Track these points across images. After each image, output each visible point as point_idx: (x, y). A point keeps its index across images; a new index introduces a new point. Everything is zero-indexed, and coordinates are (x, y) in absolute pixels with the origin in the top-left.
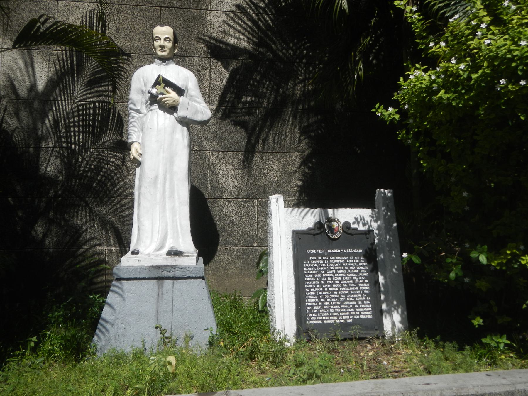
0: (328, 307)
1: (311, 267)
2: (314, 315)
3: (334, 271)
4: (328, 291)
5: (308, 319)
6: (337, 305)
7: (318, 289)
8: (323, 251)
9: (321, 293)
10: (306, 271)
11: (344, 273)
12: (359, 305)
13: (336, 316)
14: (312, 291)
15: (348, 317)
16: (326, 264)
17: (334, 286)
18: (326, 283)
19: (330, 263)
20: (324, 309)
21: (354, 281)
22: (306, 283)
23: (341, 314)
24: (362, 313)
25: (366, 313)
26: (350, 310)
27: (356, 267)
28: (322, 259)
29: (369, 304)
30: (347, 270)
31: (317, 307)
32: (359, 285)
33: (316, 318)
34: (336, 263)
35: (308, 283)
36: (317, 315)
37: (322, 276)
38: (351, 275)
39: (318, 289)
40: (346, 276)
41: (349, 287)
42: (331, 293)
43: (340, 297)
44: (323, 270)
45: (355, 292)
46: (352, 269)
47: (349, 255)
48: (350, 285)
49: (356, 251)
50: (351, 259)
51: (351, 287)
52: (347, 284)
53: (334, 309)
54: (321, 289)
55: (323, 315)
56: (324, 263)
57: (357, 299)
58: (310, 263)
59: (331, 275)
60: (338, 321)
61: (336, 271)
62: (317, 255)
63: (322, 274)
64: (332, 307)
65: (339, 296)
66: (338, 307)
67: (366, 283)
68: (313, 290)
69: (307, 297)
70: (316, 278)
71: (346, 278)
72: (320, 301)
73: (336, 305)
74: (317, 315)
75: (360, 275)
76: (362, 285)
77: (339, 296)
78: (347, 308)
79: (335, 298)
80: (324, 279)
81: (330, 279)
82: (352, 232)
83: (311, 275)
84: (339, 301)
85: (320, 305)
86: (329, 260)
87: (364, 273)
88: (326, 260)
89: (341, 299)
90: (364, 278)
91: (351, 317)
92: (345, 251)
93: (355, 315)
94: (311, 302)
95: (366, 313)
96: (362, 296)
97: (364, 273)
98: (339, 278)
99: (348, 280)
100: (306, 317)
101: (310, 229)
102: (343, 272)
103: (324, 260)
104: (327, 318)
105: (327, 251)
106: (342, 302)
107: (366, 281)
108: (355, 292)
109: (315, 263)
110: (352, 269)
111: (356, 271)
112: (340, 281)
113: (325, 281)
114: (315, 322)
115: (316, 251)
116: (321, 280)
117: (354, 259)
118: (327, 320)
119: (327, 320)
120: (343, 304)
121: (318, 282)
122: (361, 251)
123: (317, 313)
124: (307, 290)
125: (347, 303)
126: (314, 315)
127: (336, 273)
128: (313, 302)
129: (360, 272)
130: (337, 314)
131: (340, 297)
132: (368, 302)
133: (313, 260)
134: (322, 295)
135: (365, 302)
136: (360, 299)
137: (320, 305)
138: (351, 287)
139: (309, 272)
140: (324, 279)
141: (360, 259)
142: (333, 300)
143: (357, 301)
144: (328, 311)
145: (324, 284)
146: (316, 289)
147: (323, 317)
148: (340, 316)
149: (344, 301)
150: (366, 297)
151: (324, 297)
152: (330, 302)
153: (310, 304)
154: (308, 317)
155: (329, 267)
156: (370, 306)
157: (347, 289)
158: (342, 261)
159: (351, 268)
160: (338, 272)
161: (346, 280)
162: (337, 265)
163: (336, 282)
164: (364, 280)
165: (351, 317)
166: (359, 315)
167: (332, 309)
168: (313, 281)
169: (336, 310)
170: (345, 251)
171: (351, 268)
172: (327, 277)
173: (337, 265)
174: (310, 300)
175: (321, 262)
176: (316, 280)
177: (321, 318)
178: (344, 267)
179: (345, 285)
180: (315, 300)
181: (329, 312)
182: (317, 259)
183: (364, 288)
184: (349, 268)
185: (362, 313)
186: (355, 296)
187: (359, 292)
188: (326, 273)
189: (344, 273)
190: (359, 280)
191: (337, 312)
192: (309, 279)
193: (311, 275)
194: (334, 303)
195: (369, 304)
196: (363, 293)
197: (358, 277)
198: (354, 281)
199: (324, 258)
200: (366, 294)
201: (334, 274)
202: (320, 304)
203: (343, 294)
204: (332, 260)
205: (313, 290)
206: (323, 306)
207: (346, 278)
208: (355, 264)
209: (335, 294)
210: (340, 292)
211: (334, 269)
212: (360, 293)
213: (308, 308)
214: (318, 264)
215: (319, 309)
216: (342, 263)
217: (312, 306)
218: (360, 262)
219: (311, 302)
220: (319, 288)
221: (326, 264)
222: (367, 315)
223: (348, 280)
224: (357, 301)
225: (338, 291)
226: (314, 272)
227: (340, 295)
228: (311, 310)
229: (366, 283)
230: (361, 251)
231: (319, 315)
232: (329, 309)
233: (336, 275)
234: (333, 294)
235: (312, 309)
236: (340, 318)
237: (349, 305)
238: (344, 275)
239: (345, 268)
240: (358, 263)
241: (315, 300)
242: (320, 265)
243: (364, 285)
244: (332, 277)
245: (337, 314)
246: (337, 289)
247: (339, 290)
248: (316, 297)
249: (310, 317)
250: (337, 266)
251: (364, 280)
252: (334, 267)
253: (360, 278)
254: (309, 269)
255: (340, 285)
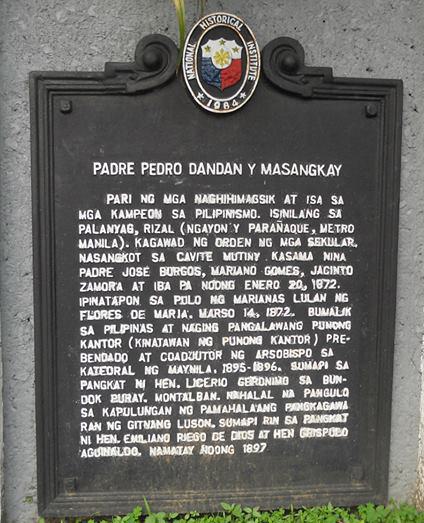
0: (172, 397)
1: (110, 237)
2: (111, 426)
3: (209, 255)
4: (177, 333)
5: (84, 440)
6: (210, 390)
7: (134, 328)
8: (167, 168)
9: (147, 343)
10: (86, 251)
11: (249, 263)
12: (299, 390)
13: (198, 430)
14: (109, 336)
15: (250, 434)
16: (175, 224)
17: (202, 314)
18: (168, 304)
19: (191, 219)
20: (151, 402)
21: (289, 294)
22: (83, 302)
23: (223, 423)
24: (307, 419)
25: (323, 419)
26: (260, 409)
27: (304, 237)
28: (158, 204)
29: (340, 386)
30: (265, 252)
31: (127, 398)
32: (311, 312)
33: (120, 437)
34: (221, 220)
35: (94, 301)
36: (124, 425)
37: (155, 276)
38: (279, 271)
39: (134, 328)
40: (260, 276)
41: (268, 321)
42: (187, 342)
43: (227, 358)
44: (159, 250)
45: (288, 340)
46: (285, 249)
47: (278, 186)
48: (271, 312)
49: (311, 170)
50: (287, 207)
51: (276, 320)
52: (261, 308)
53: (196, 406)
54: (148, 328)
55: (147, 425)
56: (167, 219)
57: (294, 366)
58: (107, 220)
59: (196, 271)
60: (206, 450)
61: (218, 253)
62: (136, 185)
63: (155, 268)
64: (186, 397)
65: (219, 354)
66: (214, 396)
67: (341, 305)
68: (112, 328)
69: (85, 358)
70: (128, 283)
71: (258, 285)
72: (140, 375)
73: (203, 390)
74: (124, 425)
75: (319, 270)
76: (323, 312)
77: (219, 354)
78: (248, 403)
79: (204, 363)
80: (160, 286)
81: (188, 285)
82: (305, 90)
83: (102, 271)
84: (219, 375)
85: (139, 391)
86: (190, 207)
87: (336, 263)
88: (179, 206)
89: (227, 368)
90: (332, 284)
91: (263, 434)
92: (266, 170)
93: (282, 425)
94: (99, 378)
95: (323, 419)
96: (317, 357)
97: (336, 263)
98: (229, 285)
99: (265, 292)
100: (77, 433)
101: (114, 71)
102: (249, 257)
103: (167, 209)
104: (165, 438)
105: (186, 169)
106: (233, 379)
107: (340, 298)
108: (288, 340)
109: (126, 221)
110: (285, 249)
111: (302, 257)
112: (228, 295)
113: (168, 297)
114: (113, 452)
115: (137, 168)
116: (149, 290)
117: (299, 206)
118: (161, 445)
119: (161, 445)
120: (233, 386)
121: (136, 300)
122: (334, 170)
123: (124, 420)
124: (83, 331)
125: (252, 381)
126: (111, 426)
127: (218, 260)
128: (109, 378)
129: (319, 260)
130: (207, 423)
131: (227, 358)
132: (338, 379)
133: (119, 207)
134: (148, 349)
135: (327, 380)
136: (307, 366)
137: (139, 391)
138: (276, 320)
139: (98, 254)
140: (160, 286)
141: (327, 205)
142: (196, 369)
143: (294, 376)
144: (169, 411)
145: (159, 307)
146: (124, 328)
147: (145, 433)
148: (218, 429)
149: (239, 374)
150: (332, 361)
151: (155, 360)
152: (180, 379)
153: (98, 385)
154: (85, 434)
155: (189, 238)
156: (346, 392)
157: (258, 327)
158: (247, 214)
159: (283, 243)
160: (226, 257)
161: (256, 292)
162: (224, 228)
163: (214, 300)
164: (331, 294)
165: (263, 434)
166: (297, 428)
167: (186, 403)
168: (112, 293)
169: (203, 408)
170: (266, 170)
171: (283, 243)
172: (174, 281)
173: (224, 228)
174: (100, 371)
175: (157, 214)
176: (127, 291)
177: (138, 439)
178: (255, 237)
179: (251, 313)
180: (116, 371)
181: (175, 417)
182: (136, 204)
183: (330, 325)
184: (276, 242)
185: (307, 419)
186: (290, 354)
187: (307, 339)
188: (171, 260)
189: (249, 263)
190: (312, 292)
191: (205, 416)
192: (98, 288)
193: (102, 271)
194: (197, 383)
195: (340, 386)
196: (323, 343)
197: (307, 281)
198: (289, 294)
199: (167, 200)
200: (336, 346)
201: (205, 266)
202: (140, 384)
203: (238, 347)
204: (203, 206)
205: (112, 328)
206: (150, 391)
207: (258, 285)
208: (304, 228)
209: (206, 348)
210: (225, 340)
211: (211, 246)
212: (310, 346)
213: (87, 399)
214: (138, 223)
215: (135, 406)
216: (244, 222)
217: (106, 395)
218: (324, 219)
219: (99, 378)
220: (137, 322)
221: (175, 224)
222: (329, 425)
223: (265, 292)
224: (294, 376)
225: (217, 337)
226: (120, 258)
227: (227, 350)
228: (97, 408)
229: (341, 305)
230: (334, 170)
231: (132, 425)
232: (176, 405)
233: (214, 272)
234: (194, 346)
235: (106, 401)
236: (219, 436)
237: (257, 389)
238: (249, 271)
239: (255, 242)
240: (314, 224)
241: (116, 371)
242: (147, 228)
243: (332, 312)
244: (195, 281)
245: (207, 423)
246: (214, 328)
247: (224, 330)
248: (123, 358)
249: (93, 434)
250: (222, 235)
251: (331, 294)
252: (211, 237)
253: (318, 284)
254: (102, 244)
255: (228, 313)
